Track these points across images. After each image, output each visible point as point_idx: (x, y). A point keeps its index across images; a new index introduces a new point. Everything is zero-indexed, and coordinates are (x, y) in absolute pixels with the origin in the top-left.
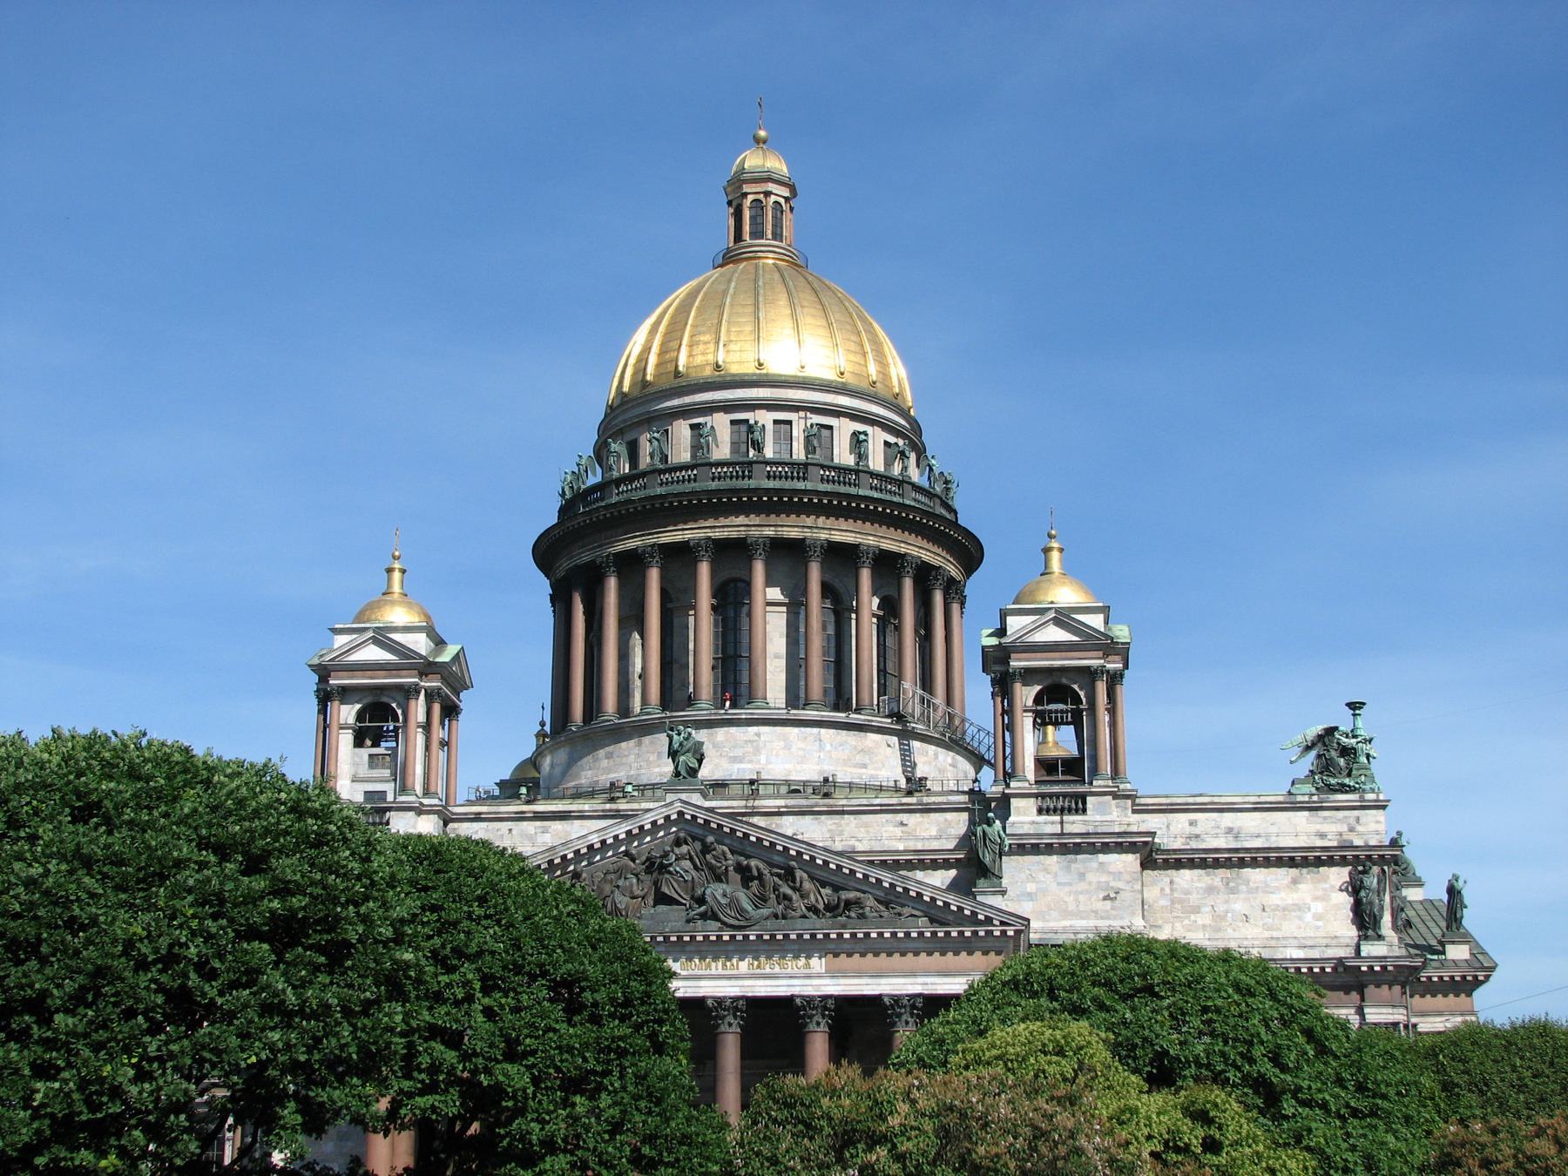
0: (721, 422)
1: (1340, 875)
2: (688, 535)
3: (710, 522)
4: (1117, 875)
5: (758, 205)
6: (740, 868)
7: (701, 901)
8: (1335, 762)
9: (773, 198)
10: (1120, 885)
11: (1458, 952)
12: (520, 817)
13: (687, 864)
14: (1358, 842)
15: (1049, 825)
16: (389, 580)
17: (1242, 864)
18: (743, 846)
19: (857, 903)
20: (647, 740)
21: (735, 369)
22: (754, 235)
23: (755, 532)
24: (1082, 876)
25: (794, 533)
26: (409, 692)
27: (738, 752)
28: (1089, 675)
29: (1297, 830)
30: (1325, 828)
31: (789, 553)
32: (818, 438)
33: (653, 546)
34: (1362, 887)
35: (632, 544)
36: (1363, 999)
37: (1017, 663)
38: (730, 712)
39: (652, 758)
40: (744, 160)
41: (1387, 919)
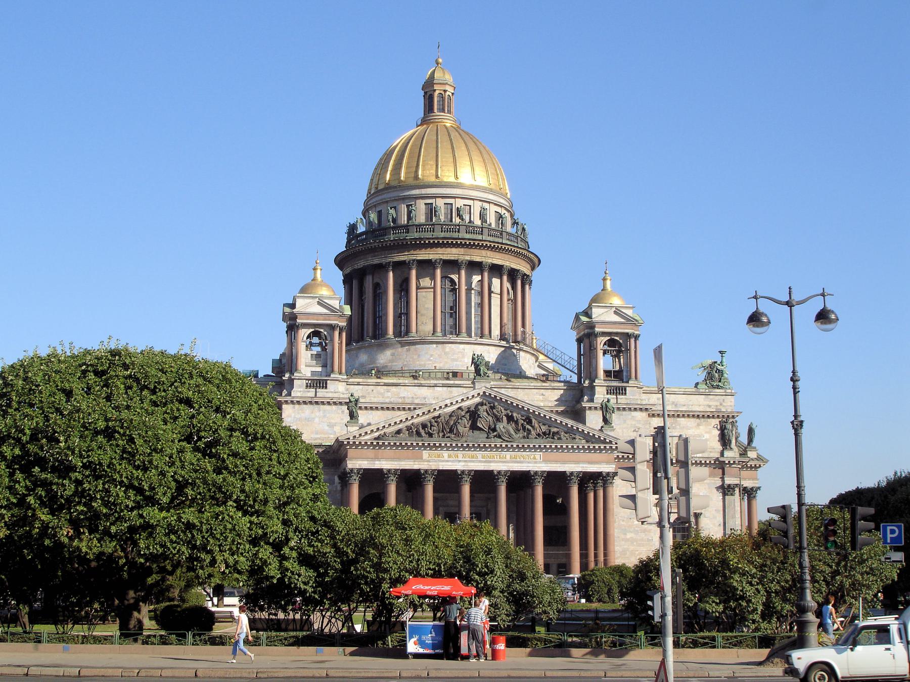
0: (440, 203)
1: (716, 422)
2: (431, 257)
3: (440, 250)
4: (639, 421)
5: (441, 96)
6: (507, 416)
7: (494, 430)
8: (714, 377)
9: (448, 93)
10: (640, 426)
11: (752, 454)
12: (378, 385)
13: (485, 413)
14: (723, 410)
15: (612, 397)
16: (315, 274)
17: (678, 416)
18: (508, 405)
19: (558, 433)
20: (412, 348)
21: (445, 180)
22: (443, 111)
23: (461, 258)
24: (625, 421)
25: (478, 259)
26: (332, 328)
27: (456, 356)
28: (628, 336)
29: (700, 403)
30: (711, 403)
31: (475, 267)
32: (482, 217)
33: (414, 260)
34: (725, 428)
35: (402, 258)
36: (723, 474)
37: (597, 330)
38: (453, 338)
39: (415, 357)
40: (434, 72)
41: (733, 441)
